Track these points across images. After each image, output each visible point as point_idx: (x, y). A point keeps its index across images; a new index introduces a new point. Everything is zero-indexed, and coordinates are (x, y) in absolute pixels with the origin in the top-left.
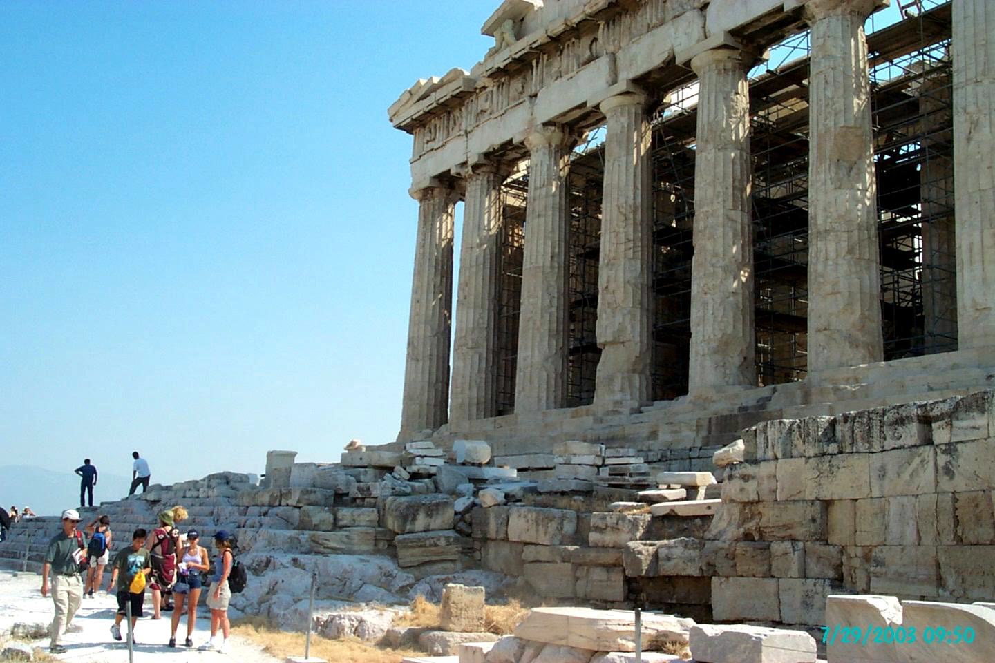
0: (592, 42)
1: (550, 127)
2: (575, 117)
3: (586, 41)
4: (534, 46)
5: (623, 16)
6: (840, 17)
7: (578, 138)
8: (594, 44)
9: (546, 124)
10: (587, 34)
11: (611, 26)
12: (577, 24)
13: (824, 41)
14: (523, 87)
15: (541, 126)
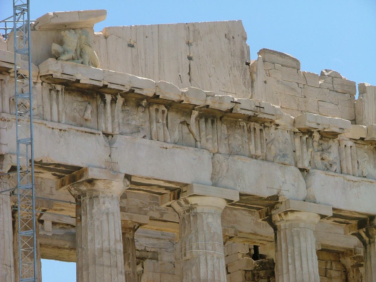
4: (137, 91)
5: (219, 123)
15: (123, 175)
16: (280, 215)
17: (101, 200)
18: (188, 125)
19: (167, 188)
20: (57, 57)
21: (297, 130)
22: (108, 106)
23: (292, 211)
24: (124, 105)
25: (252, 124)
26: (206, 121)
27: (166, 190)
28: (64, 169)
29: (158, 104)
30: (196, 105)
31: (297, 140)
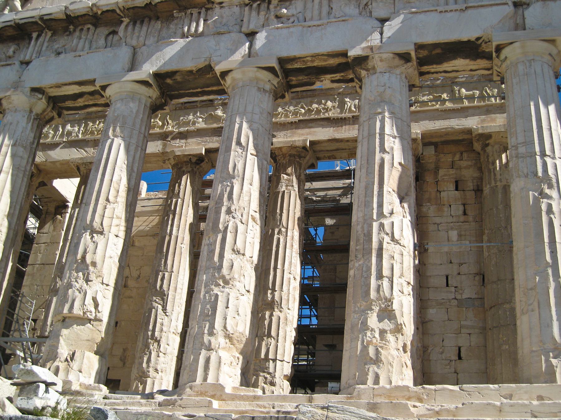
0: (110, 34)
1: (36, 94)
2: (67, 93)
3: (104, 31)
4: (45, 18)
5: (153, 22)
6: (398, 76)
7: (56, 116)
8: (111, 36)
9: (34, 90)
10: (106, 26)
11: (138, 25)
12: (103, 12)
13: (385, 90)
14: (14, 52)
15: (28, 90)
22: (33, 42)
24: (52, 36)
30: (113, 11)
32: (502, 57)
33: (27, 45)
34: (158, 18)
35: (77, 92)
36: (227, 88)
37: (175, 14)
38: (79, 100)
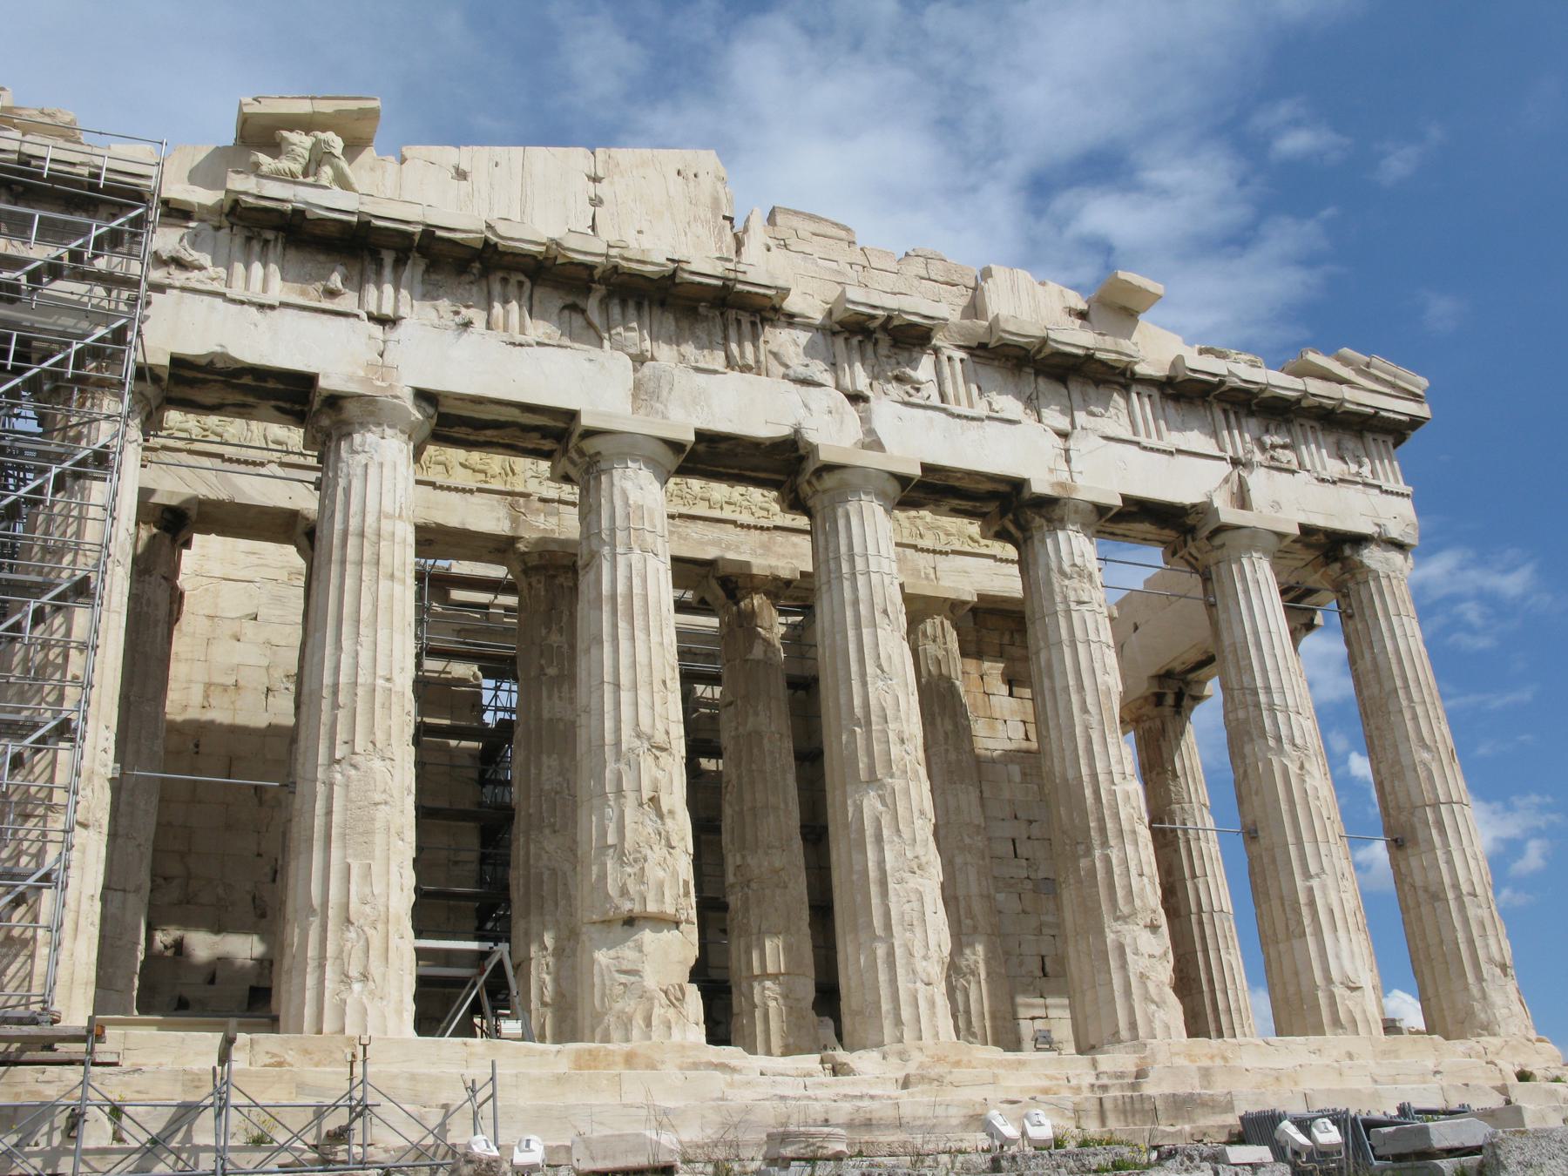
0: (565, 307)
1: (424, 404)
4: (439, 233)
5: (657, 312)
8: (566, 312)
9: (424, 397)
16: (809, 483)
17: (357, 438)
18: (583, 312)
19: (544, 432)
20: (255, 169)
21: (837, 328)
22: (388, 272)
23: (830, 468)
24: (427, 271)
25: (732, 314)
26: (624, 304)
27: (544, 437)
28: (281, 387)
29: (510, 269)
30: (591, 268)
31: (840, 342)
32: (1217, 541)
33: (373, 277)
34: (663, 304)
35: (502, 419)
36: (816, 492)
37: (701, 310)
38: (489, 432)
